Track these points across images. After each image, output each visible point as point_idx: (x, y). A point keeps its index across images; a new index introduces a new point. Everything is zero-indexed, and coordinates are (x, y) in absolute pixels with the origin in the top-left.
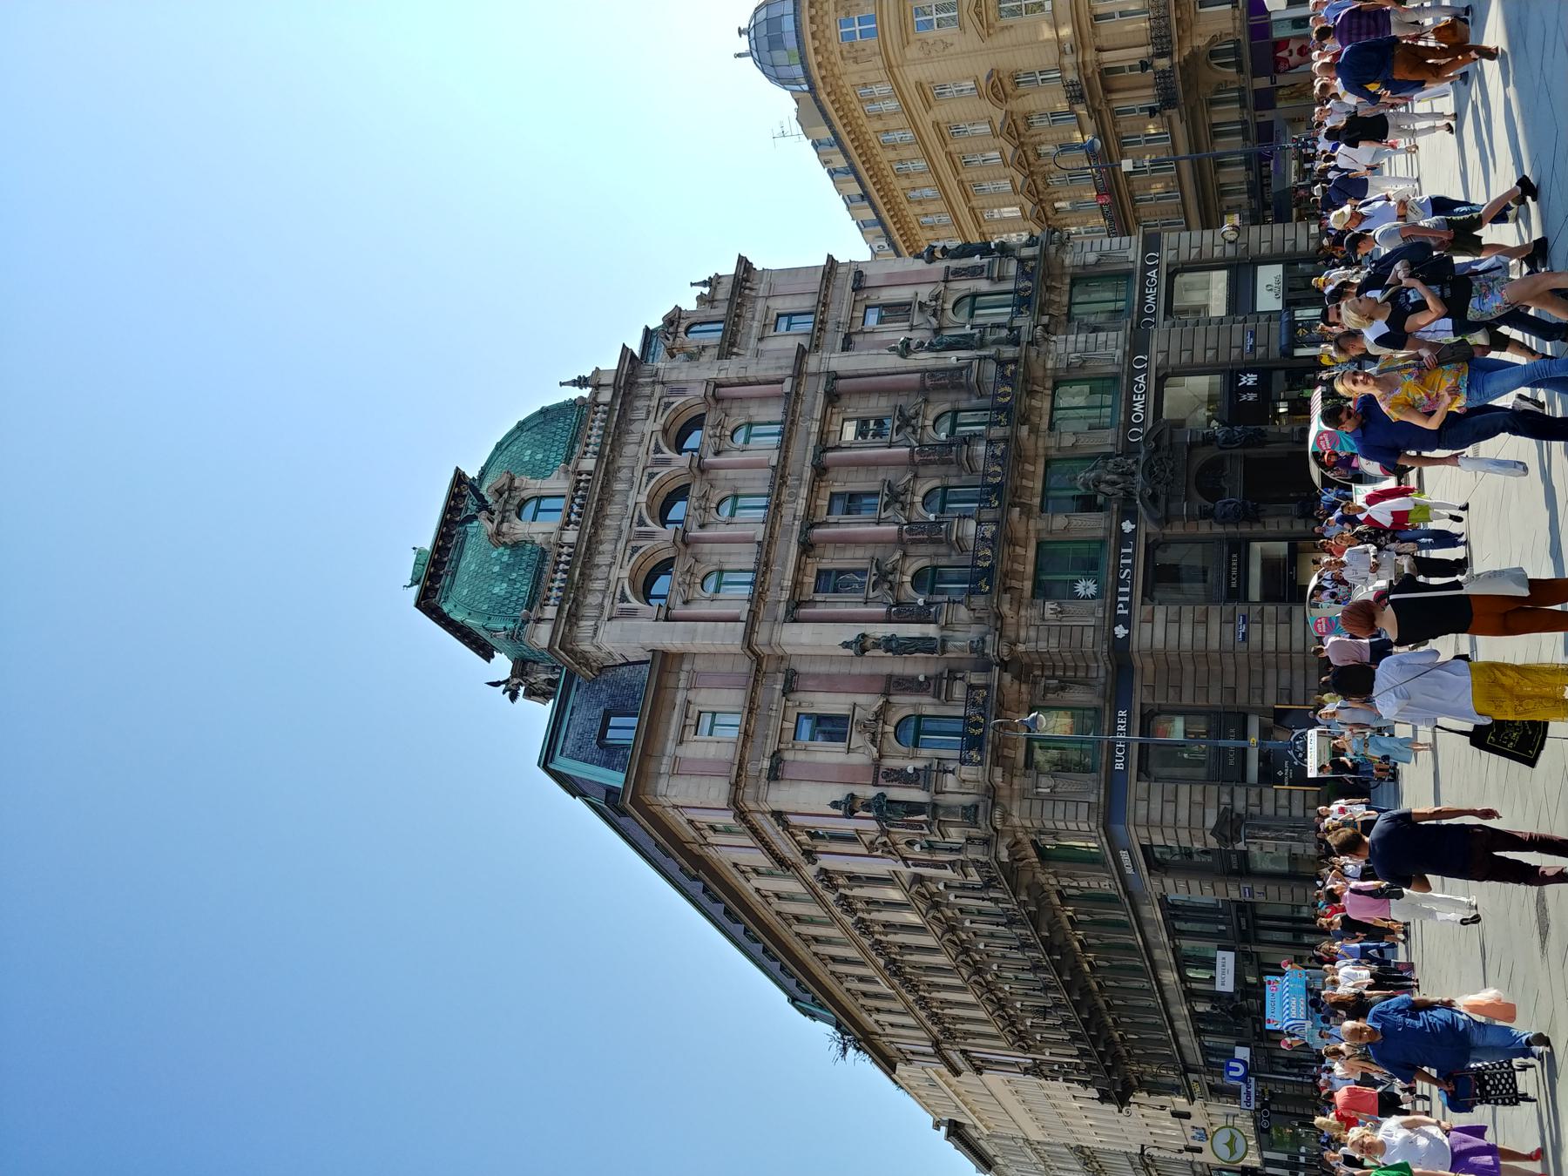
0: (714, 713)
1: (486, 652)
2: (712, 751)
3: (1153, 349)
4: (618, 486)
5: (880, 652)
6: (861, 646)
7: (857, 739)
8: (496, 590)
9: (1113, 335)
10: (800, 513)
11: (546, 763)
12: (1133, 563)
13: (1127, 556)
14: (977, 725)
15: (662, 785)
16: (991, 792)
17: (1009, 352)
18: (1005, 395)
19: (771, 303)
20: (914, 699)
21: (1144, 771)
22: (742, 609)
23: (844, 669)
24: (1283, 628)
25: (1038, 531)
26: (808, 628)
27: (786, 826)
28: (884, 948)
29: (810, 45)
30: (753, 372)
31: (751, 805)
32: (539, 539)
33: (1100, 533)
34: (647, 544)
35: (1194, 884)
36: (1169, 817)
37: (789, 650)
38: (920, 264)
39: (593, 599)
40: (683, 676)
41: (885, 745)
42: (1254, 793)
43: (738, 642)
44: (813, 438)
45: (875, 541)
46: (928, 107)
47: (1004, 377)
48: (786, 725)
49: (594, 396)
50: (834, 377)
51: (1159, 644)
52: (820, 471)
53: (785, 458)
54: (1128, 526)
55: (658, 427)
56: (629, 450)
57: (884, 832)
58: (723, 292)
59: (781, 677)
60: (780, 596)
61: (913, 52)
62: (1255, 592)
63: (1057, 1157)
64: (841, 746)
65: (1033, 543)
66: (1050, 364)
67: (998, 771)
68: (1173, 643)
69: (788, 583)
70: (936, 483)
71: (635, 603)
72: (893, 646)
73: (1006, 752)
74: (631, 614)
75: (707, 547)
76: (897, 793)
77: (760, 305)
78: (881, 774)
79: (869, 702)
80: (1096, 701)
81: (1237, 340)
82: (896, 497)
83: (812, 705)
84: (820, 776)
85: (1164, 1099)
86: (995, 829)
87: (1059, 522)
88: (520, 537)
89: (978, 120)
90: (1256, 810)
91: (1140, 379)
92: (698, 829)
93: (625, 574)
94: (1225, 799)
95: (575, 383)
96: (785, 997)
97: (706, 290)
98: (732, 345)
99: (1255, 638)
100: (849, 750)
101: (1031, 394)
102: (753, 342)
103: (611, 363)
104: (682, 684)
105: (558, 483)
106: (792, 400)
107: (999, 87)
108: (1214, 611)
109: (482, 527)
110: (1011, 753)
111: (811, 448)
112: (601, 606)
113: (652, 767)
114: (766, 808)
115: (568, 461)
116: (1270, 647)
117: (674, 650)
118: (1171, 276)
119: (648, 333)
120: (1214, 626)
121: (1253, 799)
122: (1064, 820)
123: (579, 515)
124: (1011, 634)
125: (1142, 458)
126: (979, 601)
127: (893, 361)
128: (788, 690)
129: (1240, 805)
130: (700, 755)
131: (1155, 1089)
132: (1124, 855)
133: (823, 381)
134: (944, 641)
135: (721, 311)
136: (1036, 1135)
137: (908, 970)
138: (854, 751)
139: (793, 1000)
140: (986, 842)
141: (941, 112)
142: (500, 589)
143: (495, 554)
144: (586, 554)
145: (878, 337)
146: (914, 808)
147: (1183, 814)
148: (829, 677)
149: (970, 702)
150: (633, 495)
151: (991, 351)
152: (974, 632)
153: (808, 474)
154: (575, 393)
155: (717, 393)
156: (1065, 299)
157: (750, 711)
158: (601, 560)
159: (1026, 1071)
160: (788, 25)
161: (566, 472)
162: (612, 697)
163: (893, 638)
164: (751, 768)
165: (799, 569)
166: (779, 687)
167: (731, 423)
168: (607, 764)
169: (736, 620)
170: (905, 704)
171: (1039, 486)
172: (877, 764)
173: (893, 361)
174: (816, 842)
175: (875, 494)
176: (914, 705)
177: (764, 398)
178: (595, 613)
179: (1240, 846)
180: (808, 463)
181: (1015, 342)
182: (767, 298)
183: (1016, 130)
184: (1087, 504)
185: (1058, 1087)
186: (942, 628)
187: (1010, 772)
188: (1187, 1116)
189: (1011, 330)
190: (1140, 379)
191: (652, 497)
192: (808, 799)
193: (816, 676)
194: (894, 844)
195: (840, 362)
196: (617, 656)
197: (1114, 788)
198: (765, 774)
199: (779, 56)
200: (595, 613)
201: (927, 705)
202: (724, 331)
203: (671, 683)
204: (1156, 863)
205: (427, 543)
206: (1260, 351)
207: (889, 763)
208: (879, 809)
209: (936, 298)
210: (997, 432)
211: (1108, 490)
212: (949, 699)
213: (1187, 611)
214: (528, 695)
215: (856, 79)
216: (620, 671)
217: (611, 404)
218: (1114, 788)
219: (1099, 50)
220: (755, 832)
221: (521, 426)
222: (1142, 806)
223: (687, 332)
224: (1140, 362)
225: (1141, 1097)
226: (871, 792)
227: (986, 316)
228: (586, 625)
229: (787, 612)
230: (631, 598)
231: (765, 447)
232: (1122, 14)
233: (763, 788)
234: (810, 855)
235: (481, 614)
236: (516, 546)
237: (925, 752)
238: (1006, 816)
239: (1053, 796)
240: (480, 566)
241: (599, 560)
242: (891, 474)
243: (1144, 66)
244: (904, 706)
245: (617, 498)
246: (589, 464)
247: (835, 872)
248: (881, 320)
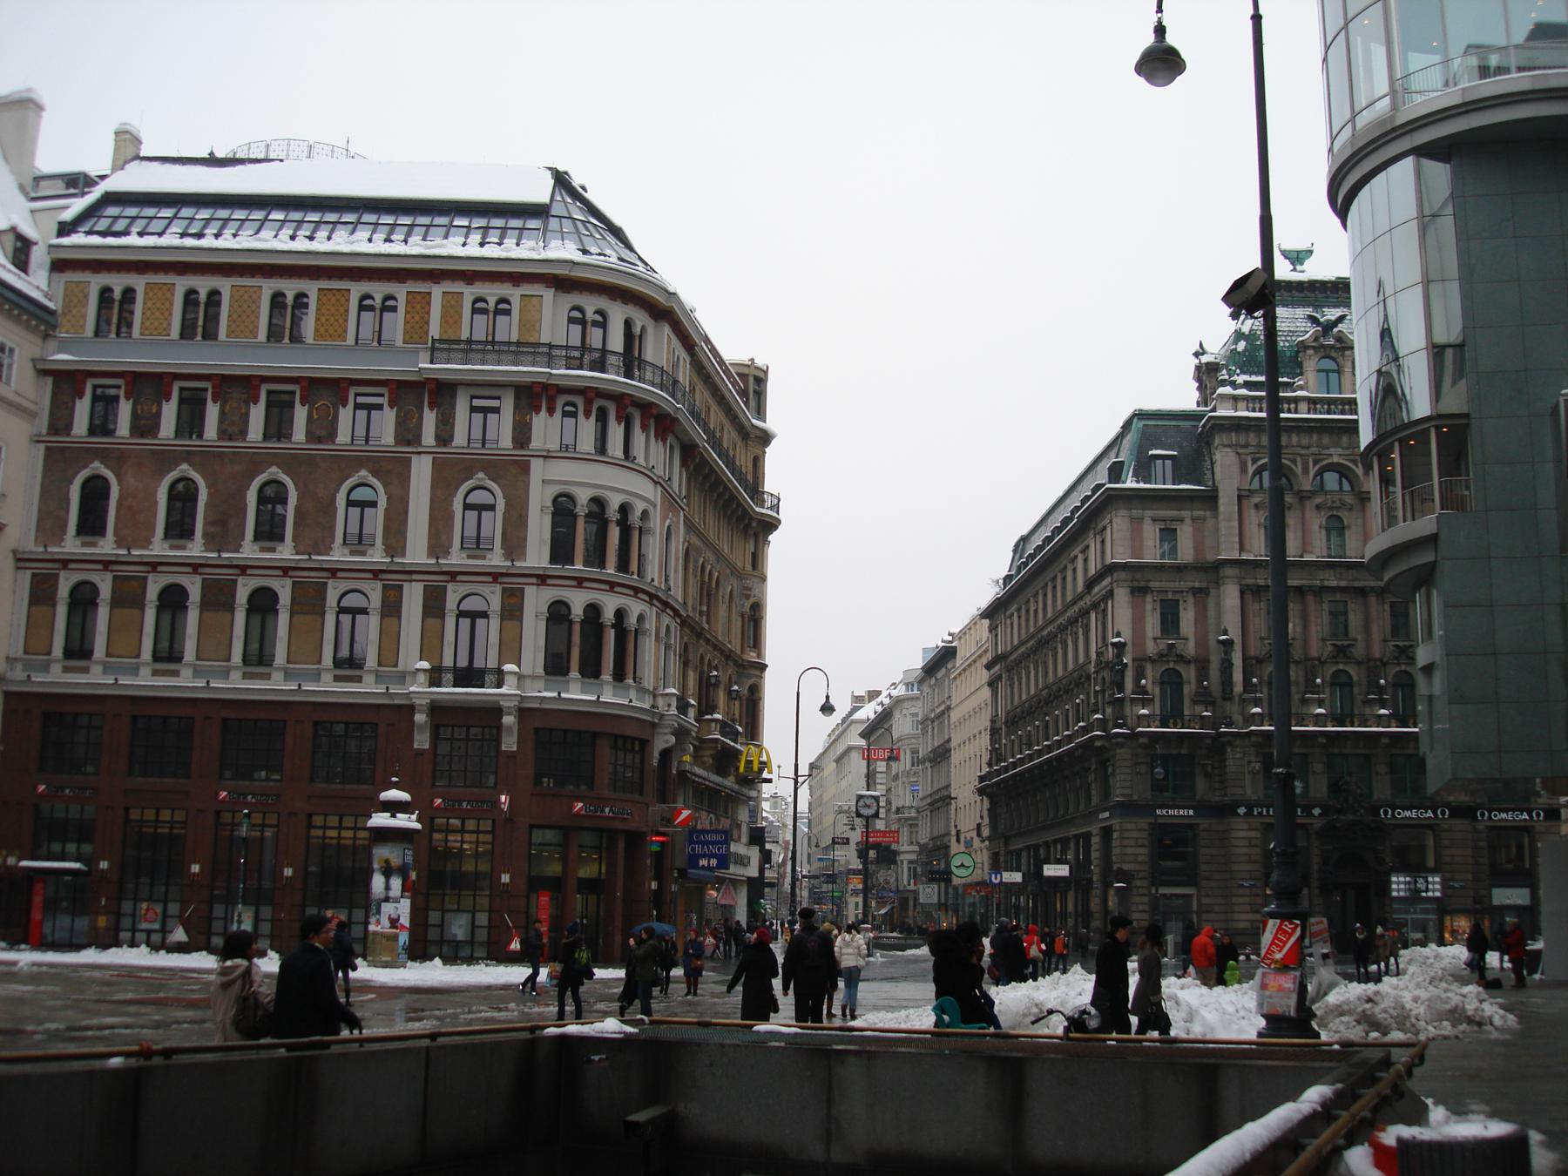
3: (1455, 822)
10: (1326, 583)
11: (1140, 415)
15: (1123, 512)
20: (1193, 681)
26: (1237, 602)
31: (1115, 576)
36: (1126, 842)
45: (1306, 642)
51: (1234, 834)
52: (1362, 592)
54: (1316, 812)
59: (1204, 585)
63: (941, 731)
70: (1355, 678)
71: (1251, 470)
72: (1227, 666)
74: (1244, 470)
75: (1298, 513)
79: (1190, 649)
80: (1198, 796)
82: (1341, 652)
84: (1138, 621)
85: (986, 820)
91: (1430, 814)
96: (1025, 532)
99: (1241, 891)
104: (1196, 513)
112: (1246, 446)
116: (1235, 900)
120: (1248, 867)
121: (1141, 891)
131: (992, 812)
132: (1107, 814)
136: (955, 715)
139: (1024, 540)
147: (1129, 851)
148: (1205, 617)
153: (1357, 584)
159: (993, 722)
166: (1197, 584)
169: (1242, 549)
170: (1189, 674)
171: (1347, 751)
178: (1242, 440)
184: (1335, 788)
185: (985, 740)
188: (979, 835)
190: (1430, 814)
192: (1121, 612)
193: (1205, 609)
197: (1144, 809)
204: (1107, 832)
207: (1149, 668)
214: (1198, 368)
218: (1144, 809)
222: (1133, 826)
224: (1443, 813)
225: (986, 804)
237: (1157, 690)
238: (1121, 745)
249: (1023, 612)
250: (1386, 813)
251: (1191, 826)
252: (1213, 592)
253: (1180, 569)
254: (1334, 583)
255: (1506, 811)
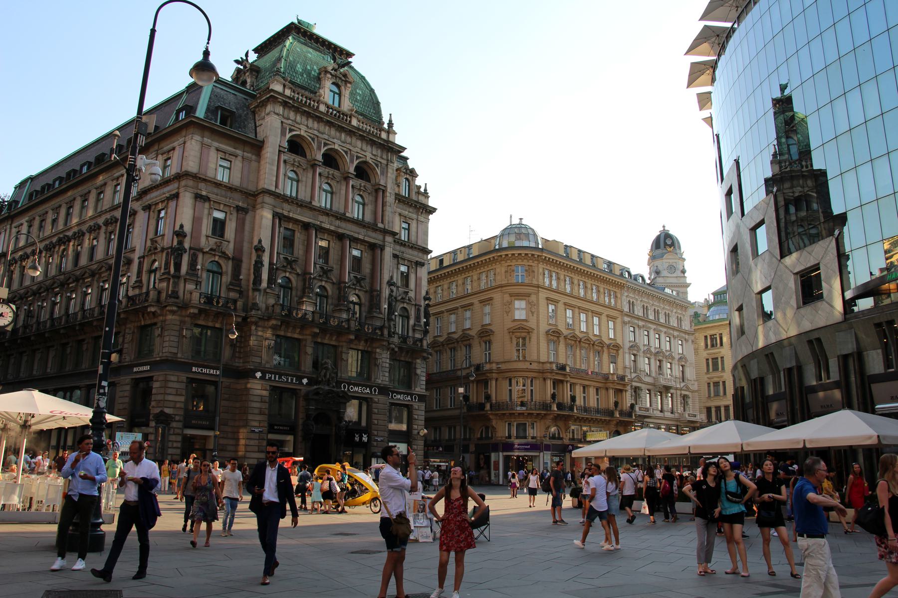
0: (230, 169)
1: (261, 50)
2: (212, 165)
3: (380, 397)
4: (343, 135)
5: (254, 258)
6: (259, 249)
7: (212, 241)
8: (299, 66)
9: (387, 379)
10: (323, 225)
12: (288, 382)
13: (292, 380)
14: (218, 302)
15: (197, 138)
16: (185, 306)
17: (386, 332)
18: (368, 329)
19: (415, 221)
21: (191, 381)
22: (280, 191)
23: (246, 238)
24: (256, 449)
25: (306, 340)
27: (169, 199)
28: (79, 237)
29: (516, 252)
30: (388, 209)
31: (183, 183)
32: (321, 91)
33: (303, 369)
34: (315, 146)
35: (127, 400)
36: (169, 391)
37: (258, 212)
38: (424, 293)
39: (292, 115)
40: (249, 155)
41: (208, 256)
42: (179, 431)
43: (266, 187)
44: (356, 235)
46: (481, 302)
47: (376, 329)
48: (222, 206)
49: (383, 130)
50: (382, 248)
53: (349, 221)
54: (305, 381)
55: (368, 159)
56: (359, 143)
57: (163, 250)
58: (422, 199)
59: (245, 206)
60: (286, 210)
61: (507, 298)
62: (271, 436)
64: (210, 233)
65: (300, 337)
66: (378, 350)
67: (196, 311)
68: (252, 398)
69: (291, 215)
70: (330, 293)
71: (288, 136)
72: (259, 264)
73: (203, 315)
74: (283, 133)
75: (310, 175)
76: (185, 259)
77: (414, 216)
78: (196, 251)
79: (230, 249)
81: (381, 433)
83: (230, 220)
84: (196, 221)
86: (166, 306)
87: (309, 350)
88: (323, 82)
89: (468, 322)
90: (172, 432)
91: (368, 391)
92: (169, 151)
93: (303, 133)
94: (177, 418)
95: (390, 121)
97: (422, 190)
98: (399, 201)
100: (207, 236)
101: (366, 341)
102: (399, 210)
103: (399, 140)
105: (346, 106)
106: (373, 227)
107: (486, 334)
108: (265, 418)
109: (330, 65)
110: (202, 318)
111: (352, 234)
112: (288, 119)
113: (207, 133)
114: (181, 190)
115: (356, 112)
117: (264, 152)
118: (407, 406)
119: (406, 159)
122: (170, 341)
123: (332, 113)
124: (260, 324)
125: (335, 389)
126: (278, 309)
127: (386, 278)
128: (238, 209)
129: (174, 424)
130: (210, 158)
133: (381, 243)
134: (259, 290)
135: (414, 197)
137: (62, 247)
138: (207, 239)
140: (158, 301)
141: (477, 306)
142: (299, 68)
143: (315, 67)
144: (312, 115)
145: (395, 270)
146: (178, 266)
147: (171, 398)
149: (228, 300)
150: (339, 142)
151: (386, 325)
152: (262, 306)
153: (340, 231)
154: (386, 120)
155: (379, 190)
156: (402, 359)
157: (231, 188)
158: (310, 122)
160: (525, 243)
161: (352, 110)
162: (240, 116)
163: (262, 265)
164: (202, 185)
165: (296, 221)
166: (240, 204)
167: (365, 195)
168: (208, 110)
169: (277, 186)
170: (228, 267)
171: (326, 341)
172: (201, 250)
173: (386, 278)
174: (156, 213)
175: (327, 262)
176: (227, 273)
177: (375, 213)
179: (153, 424)
180: (345, 232)
181: (390, 335)
182: (417, 220)
183: (465, 339)
184: (316, 364)
186: (265, 290)
187: (193, 316)
189: (394, 333)
190: (368, 391)
191: (336, 151)
192: (185, 212)
193: (243, 224)
194: (155, 253)
195: (388, 251)
196: (261, 122)
197: (185, 366)
198: (199, 192)
199: (512, 238)
200: (286, 115)
201: (226, 279)
202: (405, 197)
203: (247, 149)
205: (317, 31)
206: (375, 444)
207: (200, 256)
208: (178, 249)
209: (409, 300)
210: (352, 323)
211: (323, 373)
212: (229, 290)
213: (267, 405)
214: (238, 71)
215: (498, 270)
216: (252, 122)
217: (380, 138)
218: (185, 366)
219: (497, 380)
220: (166, 182)
221: (372, 91)
223: (407, 179)
224: (375, 391)
226: (187, 245)
227: (399, 321)
228: (280, 110)
229: (277, 213)
230: (291, 134)
231: (355, 212)
232: (510, 390)
233: (192, 190)
234: (147, 208)
235: (287, 56)
236: (318, 79)
238: (173, 312)
239: (181, 336)
240: (310, 60)
241: (310, 121)
242: (336, 272)
243: (488, 397)
244: (227, 266)
245: (338, 134)
246: (354, 122)
247: (134, 219)
248: (402, 273)
249: (36, 223)
250: (345, 387)
251: (215, 383)
252: (250, 213)
253: (231, 189)
254: (327, 226)
255: (400, 393)
